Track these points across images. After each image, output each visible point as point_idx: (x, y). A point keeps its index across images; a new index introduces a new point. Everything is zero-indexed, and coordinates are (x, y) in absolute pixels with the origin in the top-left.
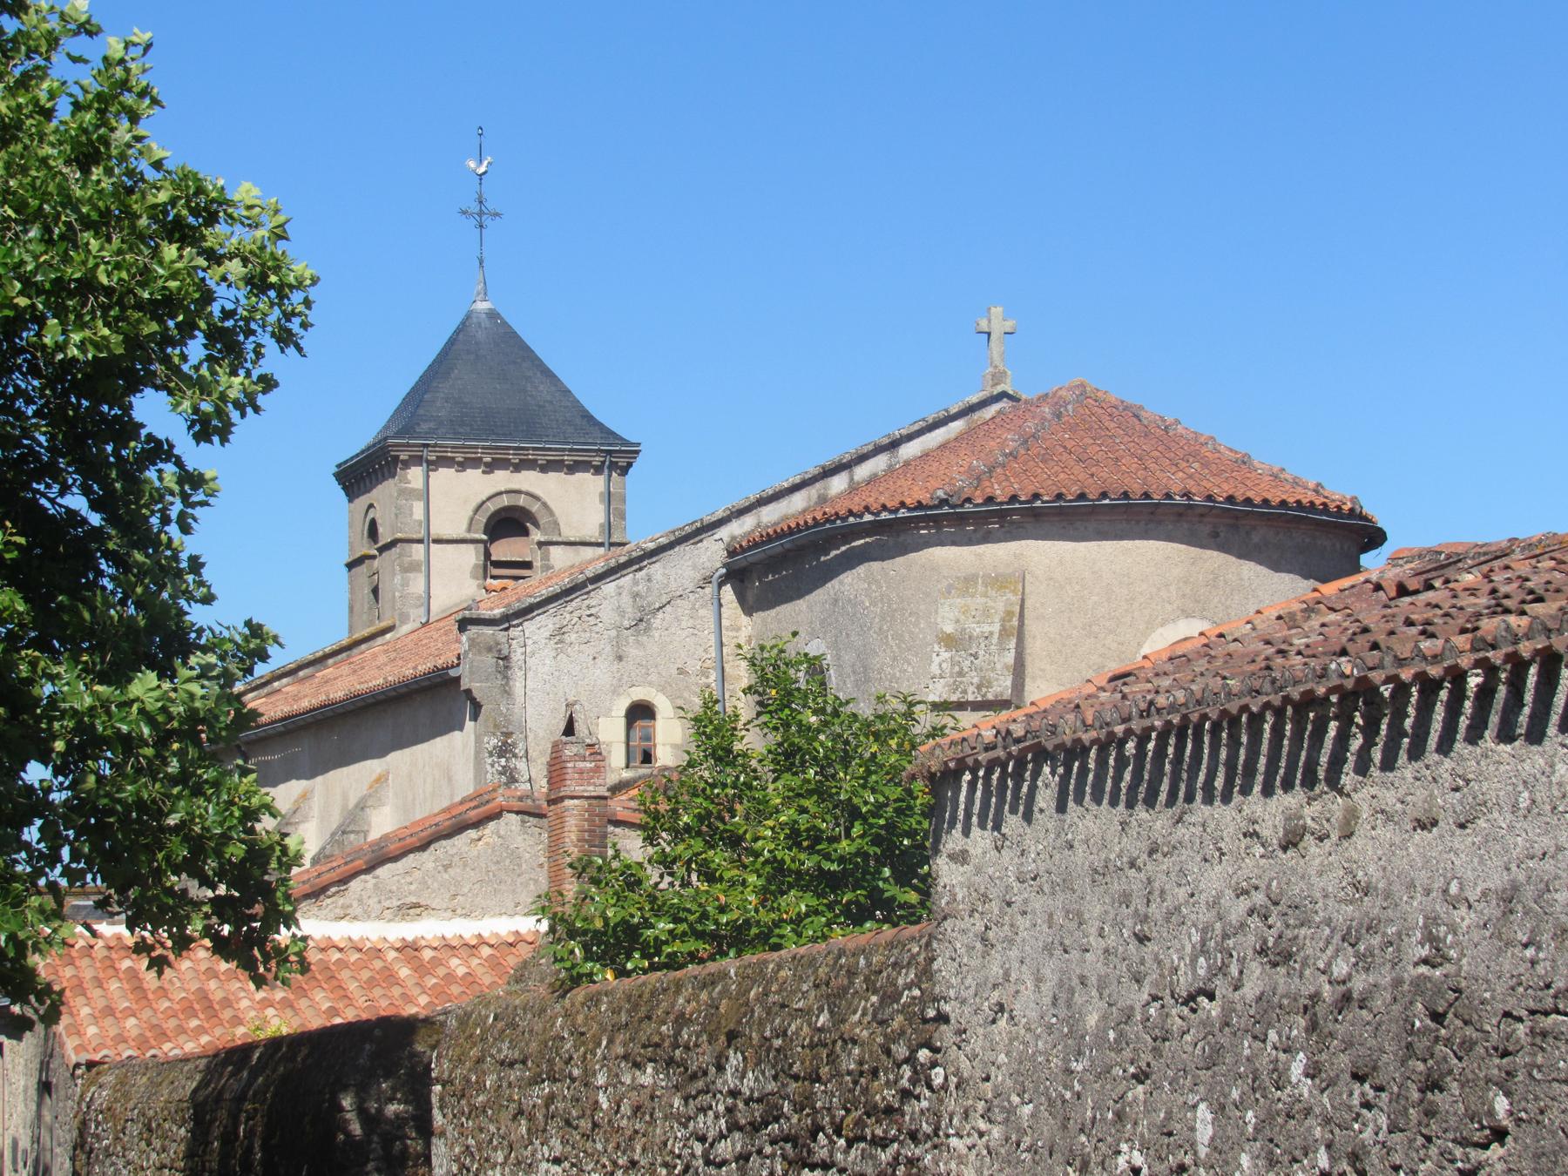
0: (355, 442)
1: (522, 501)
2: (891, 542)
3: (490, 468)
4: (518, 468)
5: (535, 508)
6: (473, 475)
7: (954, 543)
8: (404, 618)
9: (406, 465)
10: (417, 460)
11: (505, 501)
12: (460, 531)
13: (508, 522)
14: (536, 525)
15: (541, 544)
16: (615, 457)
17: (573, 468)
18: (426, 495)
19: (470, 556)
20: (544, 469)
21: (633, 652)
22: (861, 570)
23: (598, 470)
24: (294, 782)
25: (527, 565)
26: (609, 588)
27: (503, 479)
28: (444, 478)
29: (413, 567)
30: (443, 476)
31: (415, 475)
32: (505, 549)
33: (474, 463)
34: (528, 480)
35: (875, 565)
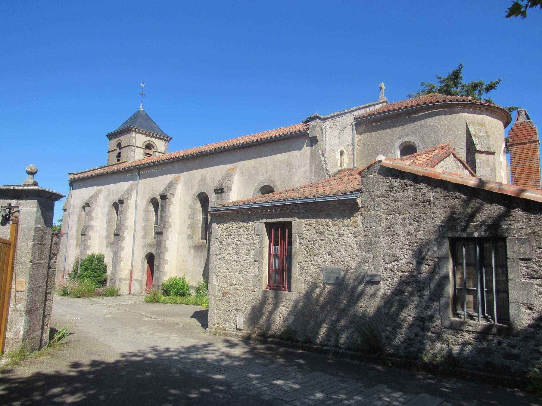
0: (113, 129)
1: (152, 143)
2: (448, 111)
3: (147, 136)
4: (152, 137)
5: (154, 145)
6: (144, 136)
7: (468, 113)
8: (130, 160)
9: (133, 131)
10: (135, 131)
11: (149, 142)
12: (141, 146)
13: (149, 146)
14: (154, 148)
15: (154, 151)
16: (168, 139)
17: (161, 139)
18: (135, 138)
19: (142, 151)
20: (156, 138)
21: (341, 137)
22: (437, 117)
23: (165, 141)
24: (95, 187)
25: (151, 155)
26: (339, 119)
27: (149, 138)
28: (139, 135)
29: (132, 151)
30: (139, 135)
31: (134, 134)
32: (148, 151)
33: (144, 134)
34: (153, 139)
35: (443, 117)
